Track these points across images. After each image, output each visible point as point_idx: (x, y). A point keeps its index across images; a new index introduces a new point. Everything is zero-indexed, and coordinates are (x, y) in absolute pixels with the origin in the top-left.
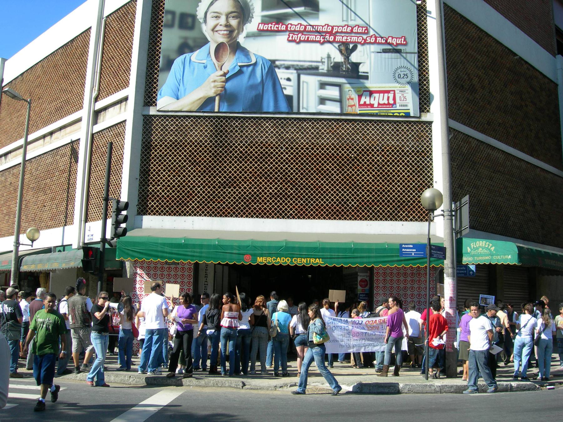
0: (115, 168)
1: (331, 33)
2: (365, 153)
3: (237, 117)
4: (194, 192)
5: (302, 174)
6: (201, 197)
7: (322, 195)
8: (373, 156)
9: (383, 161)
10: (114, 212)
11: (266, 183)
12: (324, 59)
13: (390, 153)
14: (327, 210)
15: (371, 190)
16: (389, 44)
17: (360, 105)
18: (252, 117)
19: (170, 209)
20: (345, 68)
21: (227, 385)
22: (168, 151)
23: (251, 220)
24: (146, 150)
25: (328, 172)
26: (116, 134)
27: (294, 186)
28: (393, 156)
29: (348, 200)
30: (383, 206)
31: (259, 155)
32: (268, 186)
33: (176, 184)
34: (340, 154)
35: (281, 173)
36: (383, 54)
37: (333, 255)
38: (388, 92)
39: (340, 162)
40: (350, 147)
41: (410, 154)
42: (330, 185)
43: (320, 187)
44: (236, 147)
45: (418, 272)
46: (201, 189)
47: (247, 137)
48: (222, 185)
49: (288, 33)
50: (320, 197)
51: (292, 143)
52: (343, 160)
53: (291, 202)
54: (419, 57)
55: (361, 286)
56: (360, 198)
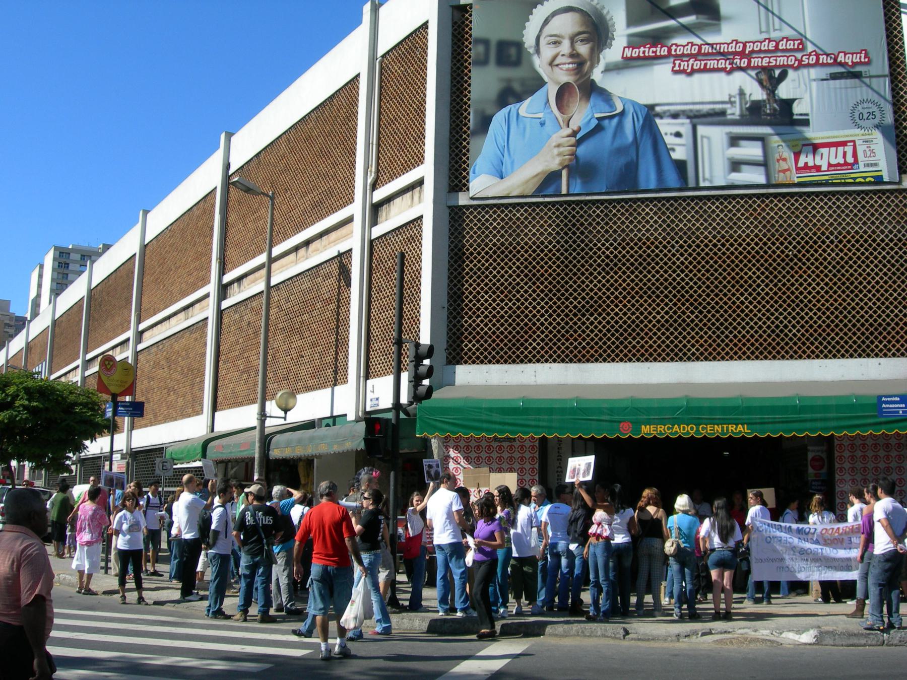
0: (409, 291)
1: (742, 54)
2: (811, 247)
3: (598, 201)
4: (534, 324)
5: (708, 287)
6: (547, 333)
7: (743, 320)
8: (824, 251)
9: (842, 258)
10: (412, 361)
11: (650, 305)
12: (734, 97)
13: (853, 246)
14: (752, 345)
15: (823, 309)
16: (841, 64)
17: (798, 169)
18: (623, 200)
19: (498, 353)
20: (770, 109)
21: (599, 633)
22: (491, 261)
23: (629, 365)
24: (456, 262)
25: (750, 282)
26: (407, 238)
27: (696, 308)
28: (858, 250)
29: (786, 327)
30: (846, 334)
31: (636, 260)
32: (654, 309)
33: (506, 312)
34: (770, 252)
35: (674, 288)
36: (832, 82)
37: (764, 418)
38: (844, 144)
39: (770, 265)
40: (786, 239)
41: (887, 245)
42: (755, 303)
43: (738, 307)
44: (599, 249)
46: (546, 320)
47: (615, 231)
48: (579, 311)
49: (672, 60)
50: (739, 324)
51: (689, 238)
52: (774, 260)
53: (693, 333)
54: (892, 82)
55: (813, 467)
56: (807, 322)
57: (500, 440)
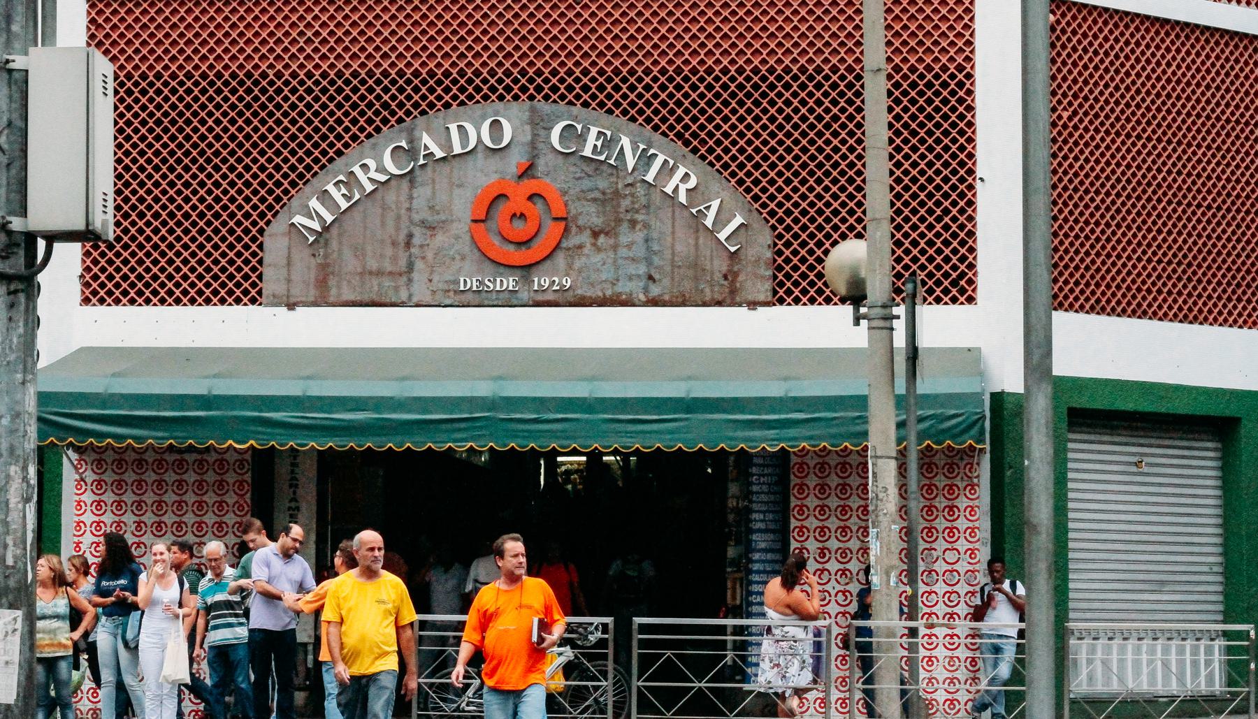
45: (927, 460)
57: (180, 451)
